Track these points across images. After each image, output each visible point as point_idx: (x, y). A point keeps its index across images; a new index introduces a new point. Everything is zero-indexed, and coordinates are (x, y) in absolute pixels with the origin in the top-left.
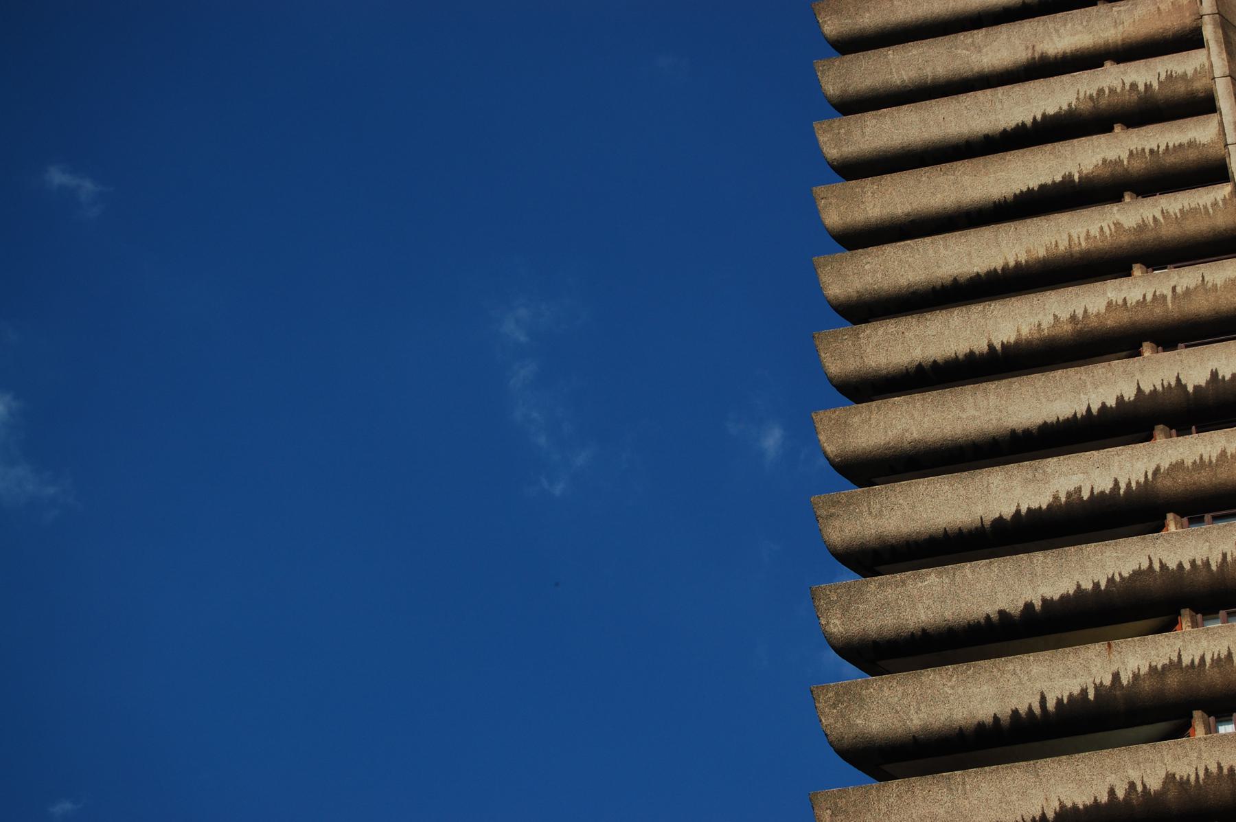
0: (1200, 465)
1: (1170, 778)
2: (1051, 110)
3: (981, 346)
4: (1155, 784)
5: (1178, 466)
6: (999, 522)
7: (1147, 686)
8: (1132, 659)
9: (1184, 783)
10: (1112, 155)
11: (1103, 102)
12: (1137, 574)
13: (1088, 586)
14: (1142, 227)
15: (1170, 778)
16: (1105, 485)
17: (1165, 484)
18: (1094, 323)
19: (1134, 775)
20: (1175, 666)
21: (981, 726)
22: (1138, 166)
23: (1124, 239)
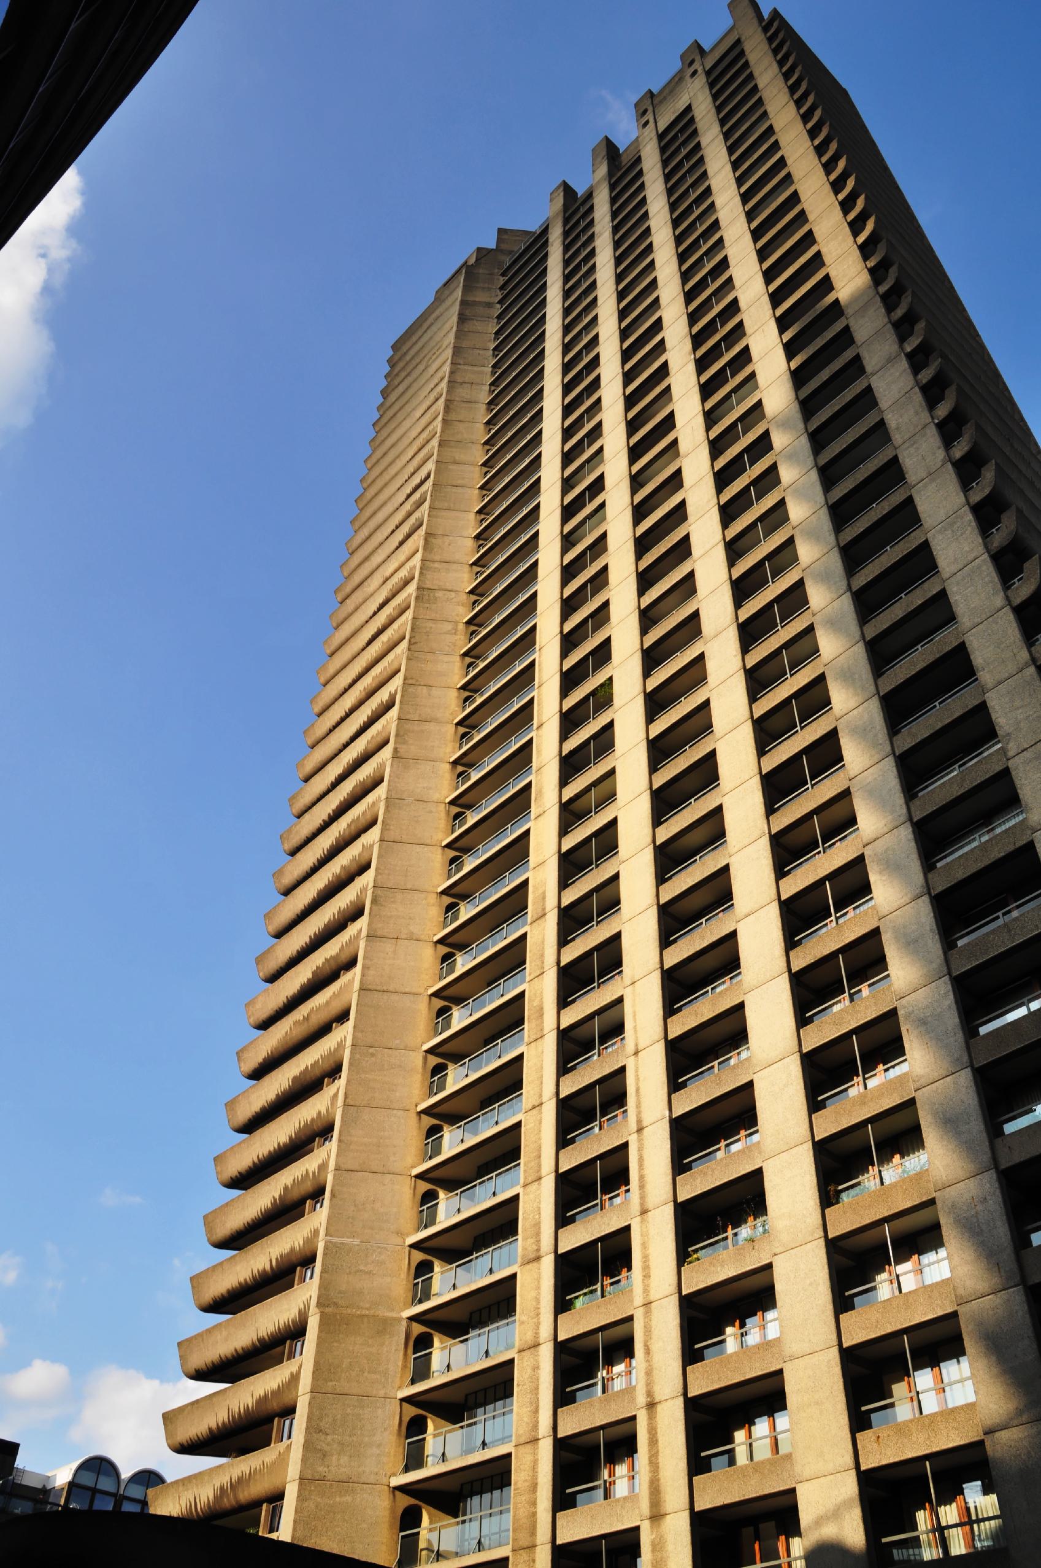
19: (333, 870)
20: (353, 821)
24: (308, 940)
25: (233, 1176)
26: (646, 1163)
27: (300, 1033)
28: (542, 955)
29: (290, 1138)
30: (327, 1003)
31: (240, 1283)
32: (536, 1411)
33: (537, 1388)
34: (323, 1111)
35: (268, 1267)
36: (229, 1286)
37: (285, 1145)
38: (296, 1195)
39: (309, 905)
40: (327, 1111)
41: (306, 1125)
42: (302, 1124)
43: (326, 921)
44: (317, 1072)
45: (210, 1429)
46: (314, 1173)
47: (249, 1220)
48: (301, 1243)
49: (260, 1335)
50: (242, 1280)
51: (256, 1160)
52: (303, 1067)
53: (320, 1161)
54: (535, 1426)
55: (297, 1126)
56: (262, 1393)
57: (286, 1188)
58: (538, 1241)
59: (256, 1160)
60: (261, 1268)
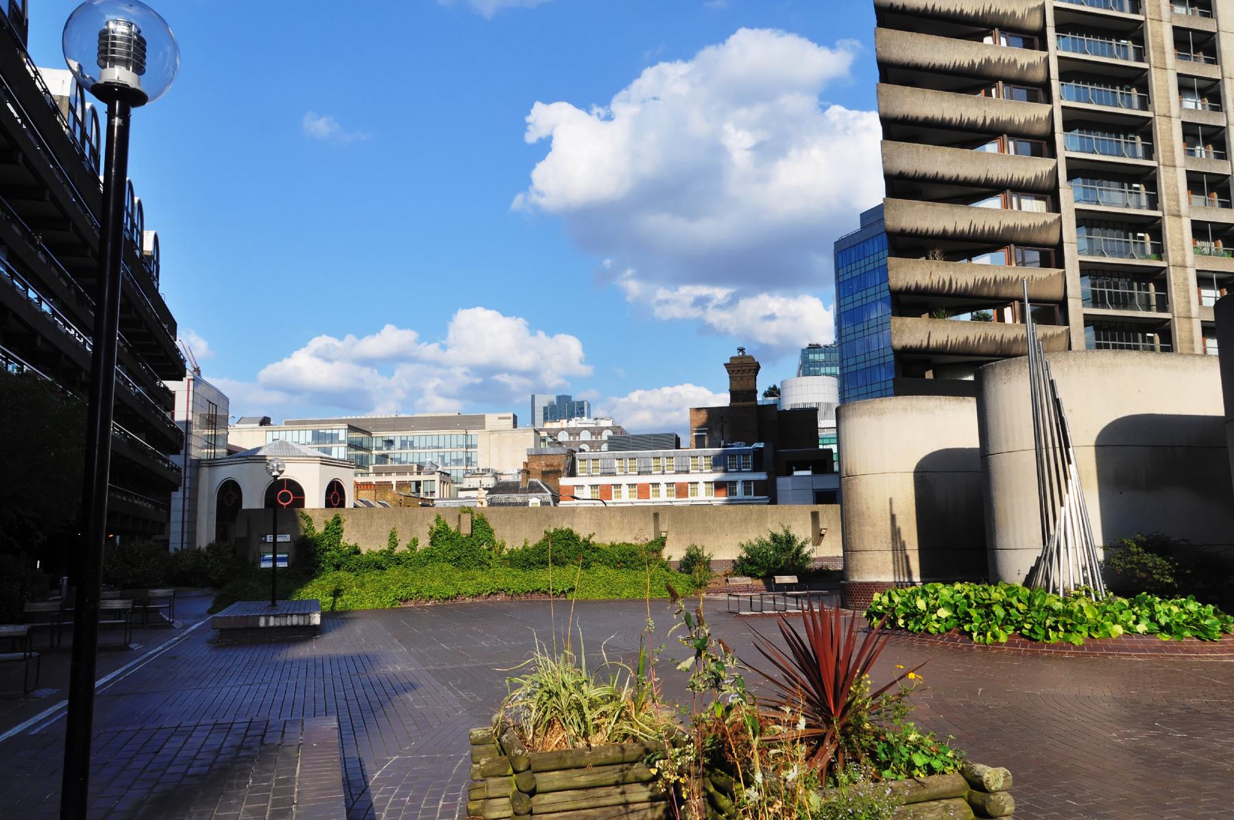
29: (977, 13)
31: (943, 119)
32: (1189, 302)
34: (1019, 14)
35: (980, 121)
36: (930, 115)
37: (968, 15)
38: (998, 71)
40: (1023, 16)
41: (997, 13)
42: (993, 10)
45: (944, 230)
46: (1022, 67)
47: (937, 64)
48: (1022, 120)
49: (990, 176)
50: (947, 117)
51: (930, 7)
53: (1031, 61)
54: (1189, 310)
55: (987, 8)
56: (1012, 224)
59: (930, 7)
60: (972, 118)
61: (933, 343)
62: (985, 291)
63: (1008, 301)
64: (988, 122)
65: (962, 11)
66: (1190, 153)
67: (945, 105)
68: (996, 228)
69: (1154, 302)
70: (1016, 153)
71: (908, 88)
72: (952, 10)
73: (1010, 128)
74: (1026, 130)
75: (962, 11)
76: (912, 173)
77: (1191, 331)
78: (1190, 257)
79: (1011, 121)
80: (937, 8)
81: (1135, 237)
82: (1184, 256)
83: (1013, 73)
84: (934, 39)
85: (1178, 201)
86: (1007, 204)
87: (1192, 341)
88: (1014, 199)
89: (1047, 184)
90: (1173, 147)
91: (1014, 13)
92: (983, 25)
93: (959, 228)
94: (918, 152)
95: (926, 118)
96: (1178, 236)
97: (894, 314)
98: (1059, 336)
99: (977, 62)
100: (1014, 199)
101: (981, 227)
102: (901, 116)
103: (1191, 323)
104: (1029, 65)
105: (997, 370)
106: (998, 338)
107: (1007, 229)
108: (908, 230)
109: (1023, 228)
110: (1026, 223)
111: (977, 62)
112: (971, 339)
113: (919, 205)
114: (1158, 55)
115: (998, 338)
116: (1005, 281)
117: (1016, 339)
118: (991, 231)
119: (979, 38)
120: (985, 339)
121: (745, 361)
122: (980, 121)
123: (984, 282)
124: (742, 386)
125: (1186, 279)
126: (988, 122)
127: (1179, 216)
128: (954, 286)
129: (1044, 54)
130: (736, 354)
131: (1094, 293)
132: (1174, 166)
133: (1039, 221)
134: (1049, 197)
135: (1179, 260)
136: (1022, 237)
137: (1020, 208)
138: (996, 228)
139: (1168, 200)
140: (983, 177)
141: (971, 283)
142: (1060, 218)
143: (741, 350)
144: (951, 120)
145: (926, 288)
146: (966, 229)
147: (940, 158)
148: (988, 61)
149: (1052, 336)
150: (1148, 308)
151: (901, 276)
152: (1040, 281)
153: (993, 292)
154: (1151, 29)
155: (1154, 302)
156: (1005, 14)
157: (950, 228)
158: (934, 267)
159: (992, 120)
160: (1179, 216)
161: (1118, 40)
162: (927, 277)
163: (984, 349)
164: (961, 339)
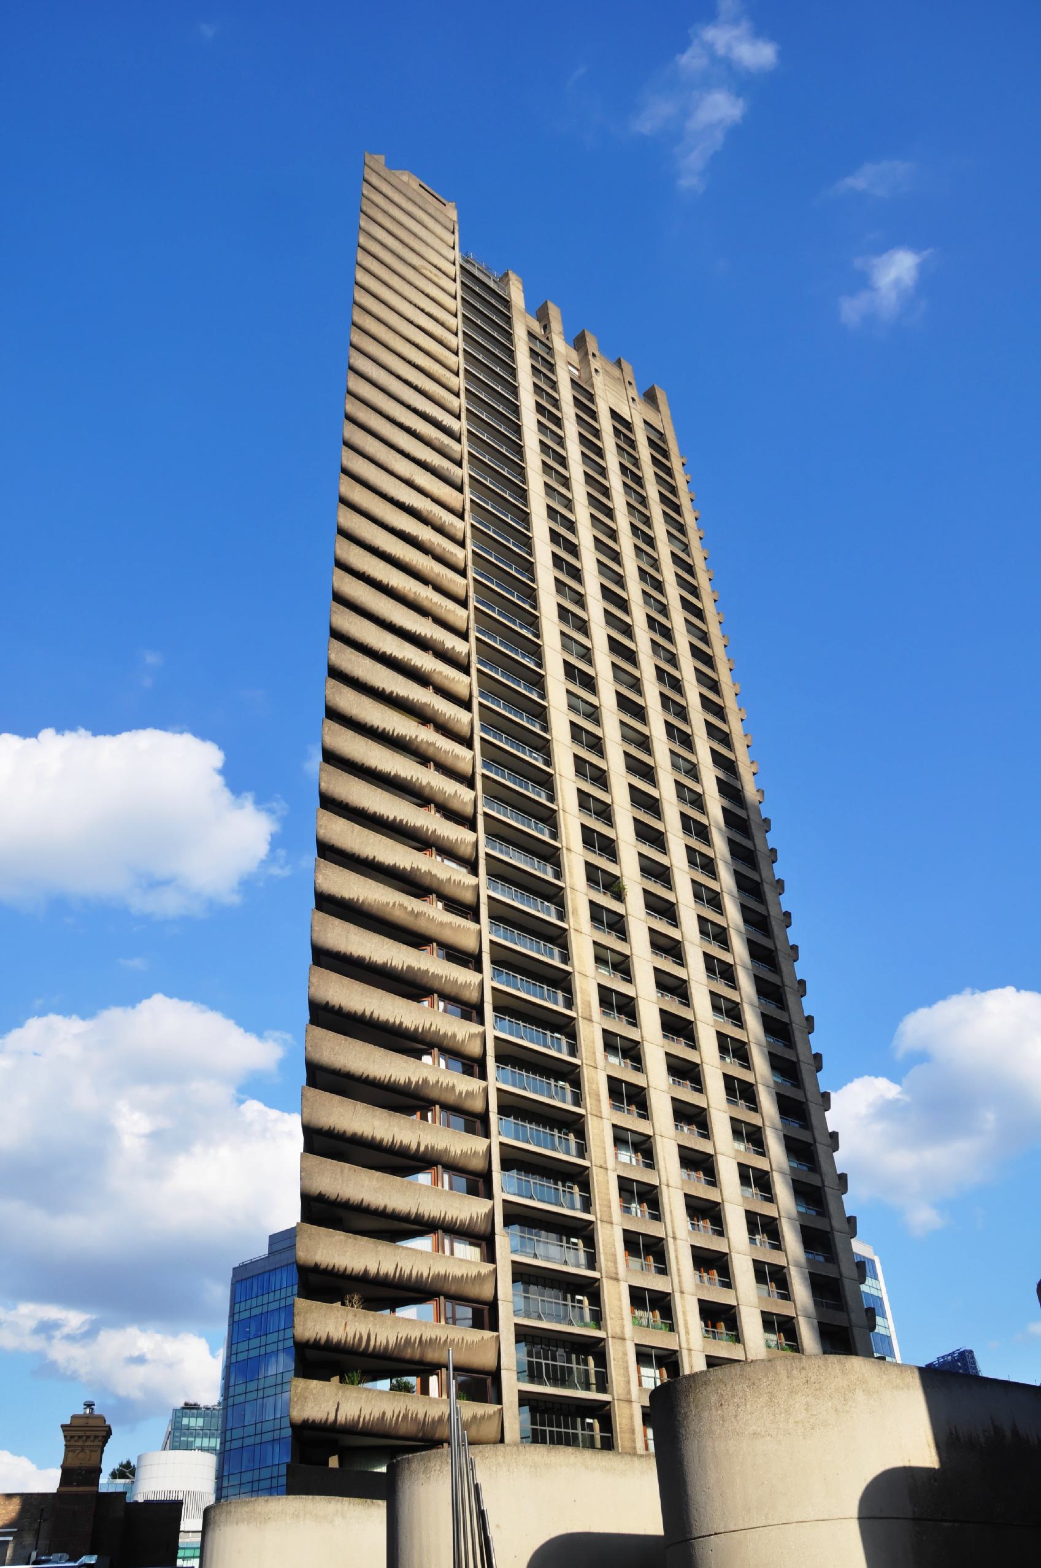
0: (446, 677)
1: (429, 783)
2: (415, 506)
3: (385, 581)
4: (424, 783)
5: (440, 673)
6: (384, 653)
7: (424, 747)
8: (425, 735)
9: (432, 788)
10: (433, 540)
11: (431, 516)
12: (425, 704)
13: (411, 698)
14: (438, 575)
15: (429, 783)
16: (419, 664)
17: (437, 678)
18: (420, 599)
19: (420, 776)
21: (372, 727)
22: (438, 551)
23: (432, 575)
24: (391, 818)
25: (331, 1003)
26: (680, 1262)
27: (399, 916)
28: (594, 1053)
29: (416, 1029)
30: (441, 924)
31: (373, 1138)
32: (628, 1382)
33: (627, 1368)
34: (460, 1037)
35: (414, 1147)
37: (407, 1029)
38: (434, 1094)
39: (380, 772)
40: (463, 1041)
41: (437, 1032)
42: (433, 1028)
43: (418, 824)
44: (436, 985)
46: (461, 1093)
47: (371, 1075)
48: (459, 1152)
49: (421, 1211)
50: (378, 1136)
52: (423, 967)
53: (470, 1089)
54: (629, 1392)
55: (427, 1025)
56: (442, 1272)
57: (425, 1081)
58: (616, 1268)
59: (368, 1013)
60: (406, 1142)
61: (341, 1418)
62: (408, 1353)
63: (434, 1368)
64: (422, 1149)
65: (401, 1023)
66: (626, 1210)
67: (377, 1123)
68: (425, 1275)
69: (593, 1380)
70: (451, 1188)
71: (338, 1098)
72: (391, 1020)
73: (445, 1159)
74: (462, 1163)
75: (401, 1023)
76: (333, 1197)
77: (632, 1417)
78: (629, 1330)
79: (446, 1151)
80: (375, 1015)
81: (573, 1300)
82: (623, 1326)
83: (451, 1099)
84: (370, 1047)
85: (615, 1262)
86: (438, 1247)
87: (633, 1431)
88: (447, 1242)
89: (482, 1227)
90: (610, 1202)
91: (454, 1036)
92: (422, 1042)
93: (383, 1271)
94: (342, 1172)
95: (354, 1135)
96: (616, 1303)
97: (297, 1375)
98: (490, 1417)
99: (414, 1080)
100: (447, 1242)
101: (407, 1272)
102: (326, 1128)
103: (631, 1408)
104: (467, 1092)
105: (414, 1465)
106: (421, 1416)
107: (437, 1277)
108: (323, 1266)
109: (454, 1278)
110: (459, 1274)
111: (414, 1080)
112: (389, 1415)
113: (339, 1236)
114: (594, 1102)
115: (421, 1416)
116: (431, 1342)
117: (441, 1418)
118: (419, 1277)
119: (417, 1054)
120: (405, 1416)
121: (91, 1422)
122: (414, 1147)
123: (408, 1341)
124: (82, 1460)
125: (625, 1354)
126: (422, 1149)
127: (617, 1280)
128: (372, 1343)
129: (483, 1083)
130: (80, 1410)
131: (530, 1363)
132: (611, 1223)
133: (473, 1272)
134: (484, 1244)
135: (618, 1330)
136: (453, 1289)
137: (452, 1253)
138: (425, 1275)
139: (606, 1260)
140: (414, 1211)
141: (392, 1342)
142: (495, 1270)
143: (89, 1405)
144: (382, 1140)
145: (339, 1342)
146: (391, 1273)
147: (366, 1182)
148: (425, 1081)
149: (483, 1417)
150: (587, 1387)
151: (310, 1324)
152: (471, 1346)
153: (417, 1355)
154: (587, 1074)
155: (593, 1380)
156: (445, 1035)
157: (373, 1270)
158: (350, 1317)
159: (427, 1147)
160: (617, 1280)
161: (556, 1081)
162: (341, 1329)
163: (403, 1430)
164: (376, 1414)
